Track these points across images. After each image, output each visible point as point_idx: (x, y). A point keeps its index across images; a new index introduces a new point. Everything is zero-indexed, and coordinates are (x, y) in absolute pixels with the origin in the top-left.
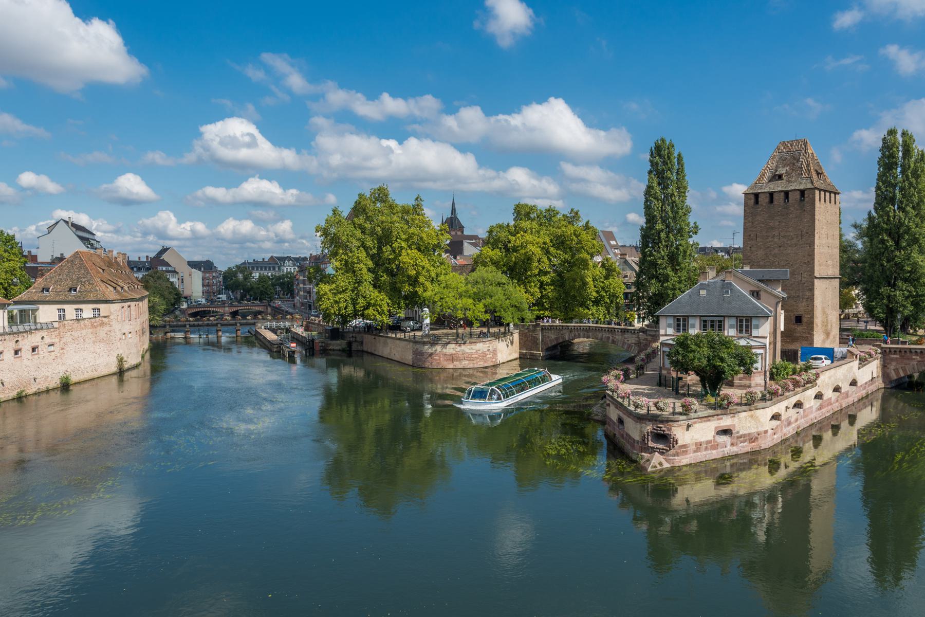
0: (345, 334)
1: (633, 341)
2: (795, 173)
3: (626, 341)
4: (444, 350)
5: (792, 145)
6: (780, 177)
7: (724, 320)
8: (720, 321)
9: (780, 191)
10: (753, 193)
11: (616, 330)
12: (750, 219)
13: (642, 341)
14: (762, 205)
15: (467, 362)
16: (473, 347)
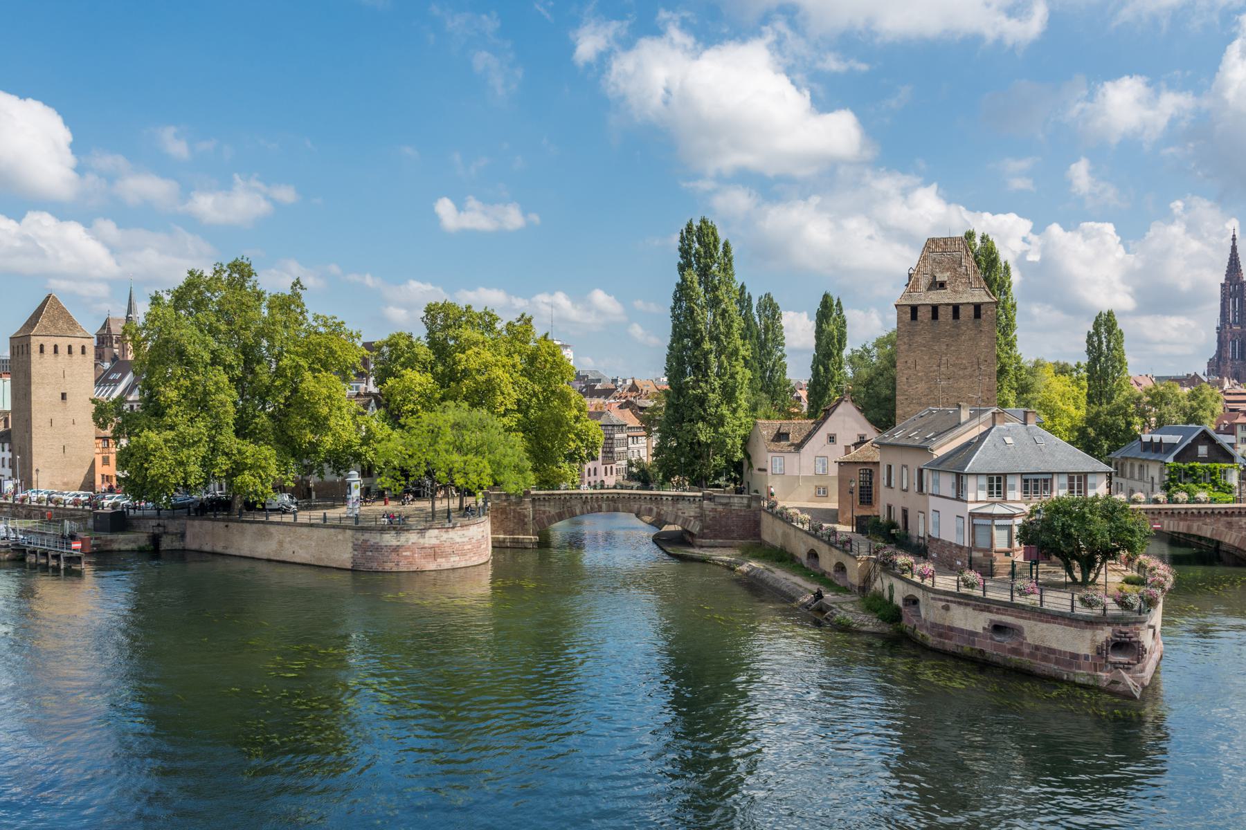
0: (135, 522)
1: (692, 514)
2: (960, 282)
3: (680, 513)
4: (421, 541)
5: (945, 243)
6: (942, 285)
7: (1052, 479)
8: (1046, 480)
9: (948, 304)
10: (909, 305)
11: (664, 498)
12: (905, 340)
13: (707, 513)
14: (922, 322)
15: (457, 558)
16: (465, 532)
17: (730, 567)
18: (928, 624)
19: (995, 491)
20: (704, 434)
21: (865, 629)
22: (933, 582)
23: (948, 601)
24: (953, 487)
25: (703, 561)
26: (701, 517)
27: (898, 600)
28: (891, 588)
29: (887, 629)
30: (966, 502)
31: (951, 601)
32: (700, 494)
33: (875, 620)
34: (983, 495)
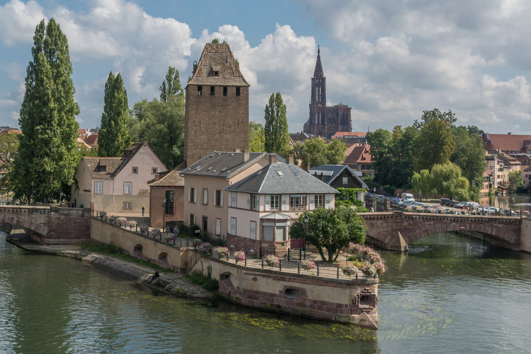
17: (76, 258)
18: (242, 291)
19: (275, 205)
20: (49, 166)
21: (196, 295)
22: (246, 263)
23: (256, 275)
24: (248, 203)
25: (54, 254)
26: (48, 223)
27: (215, 276)
28: (210, 268)
29: (210, 295)
30: (259, 212)
31: (258, 275)
32: (49, 208)
33: (201, 290)
34: (268, 208)
